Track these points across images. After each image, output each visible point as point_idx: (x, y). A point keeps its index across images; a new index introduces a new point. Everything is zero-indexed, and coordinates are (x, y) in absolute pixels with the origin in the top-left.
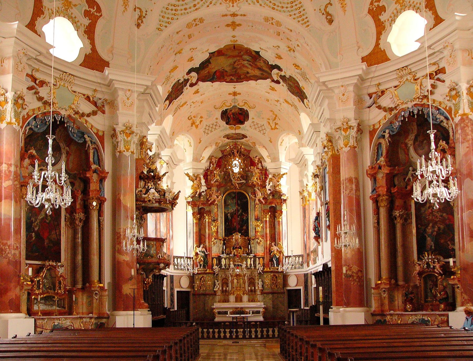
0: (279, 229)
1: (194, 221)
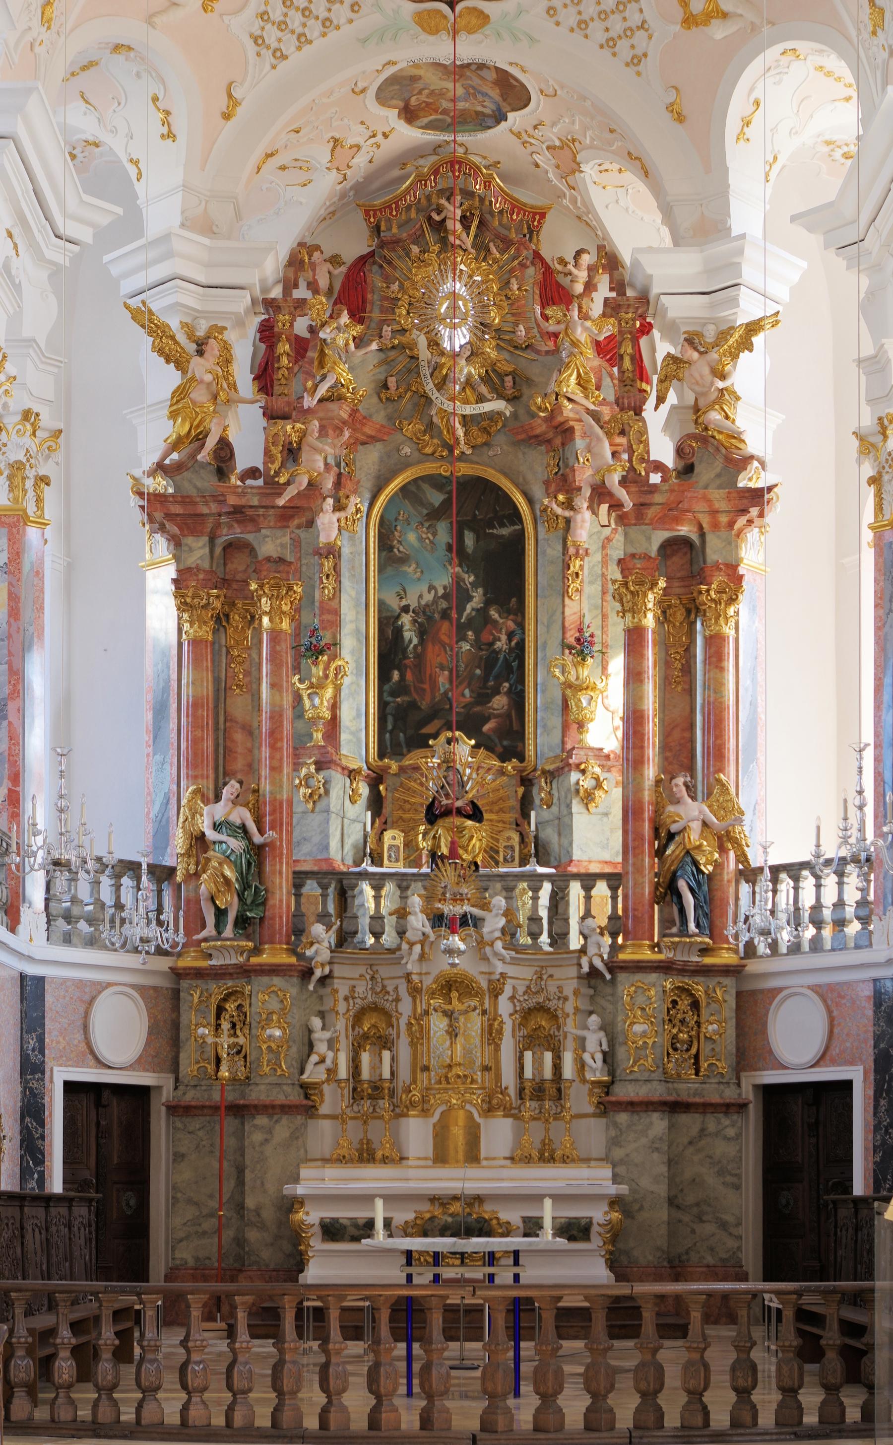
1: (186, 626)
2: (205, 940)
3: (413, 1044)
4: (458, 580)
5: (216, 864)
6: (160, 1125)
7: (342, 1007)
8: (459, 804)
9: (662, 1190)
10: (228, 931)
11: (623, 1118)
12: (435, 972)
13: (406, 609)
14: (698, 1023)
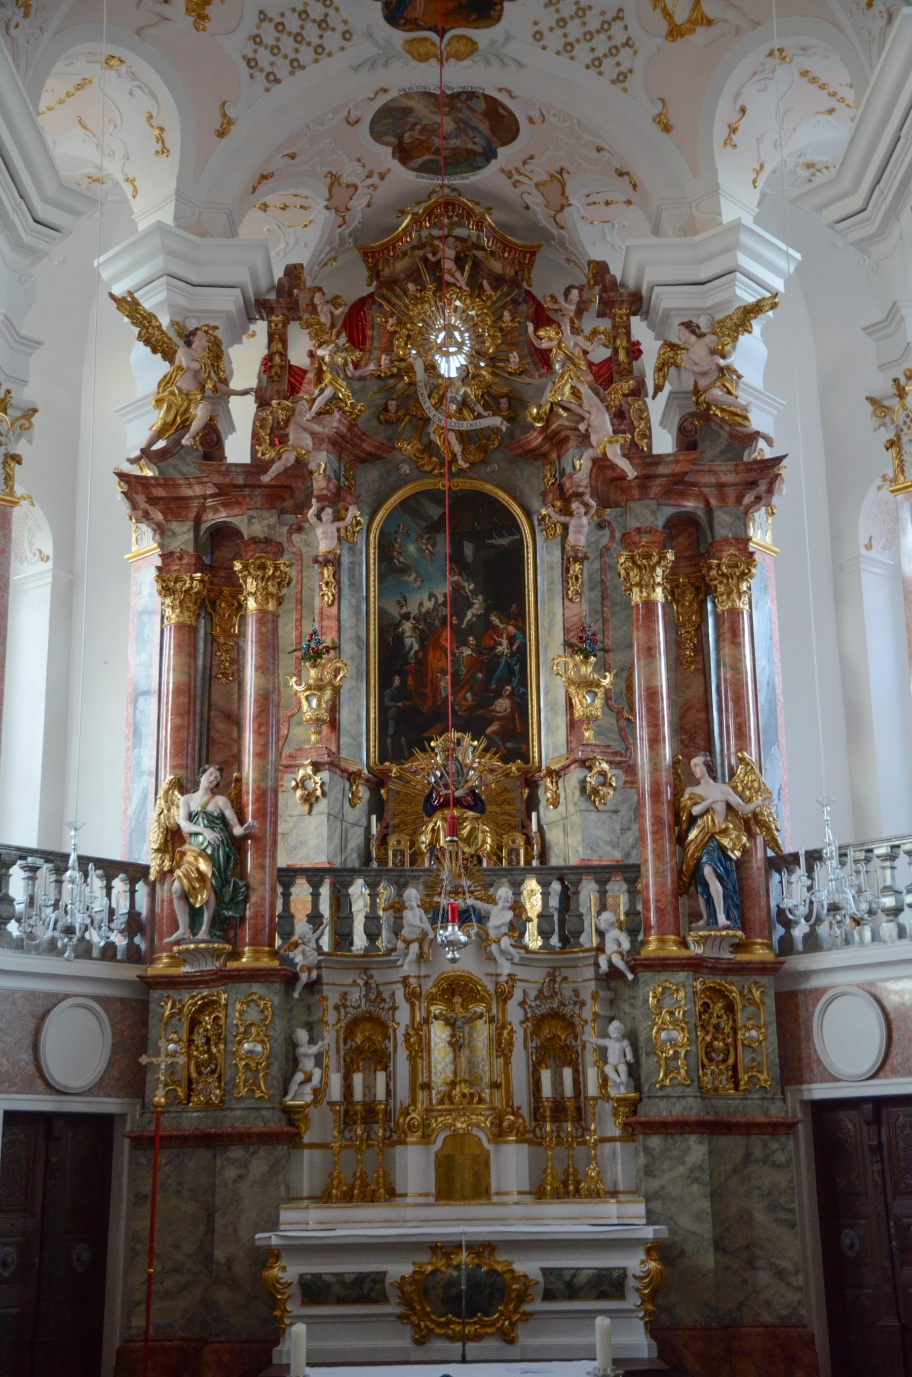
0: (737, 666)
2: (178, 943)
3: (412, 1059)
4: (457, 588)
5: (192, 859)
6: (123, 1155)
7: (331, 1017)
8: (458, 793)
9: (705, 1229)
10: (203, 933)
11: (655, 1142)
12: (435, 976)
13: (406, 617)
14: (735, 1030)
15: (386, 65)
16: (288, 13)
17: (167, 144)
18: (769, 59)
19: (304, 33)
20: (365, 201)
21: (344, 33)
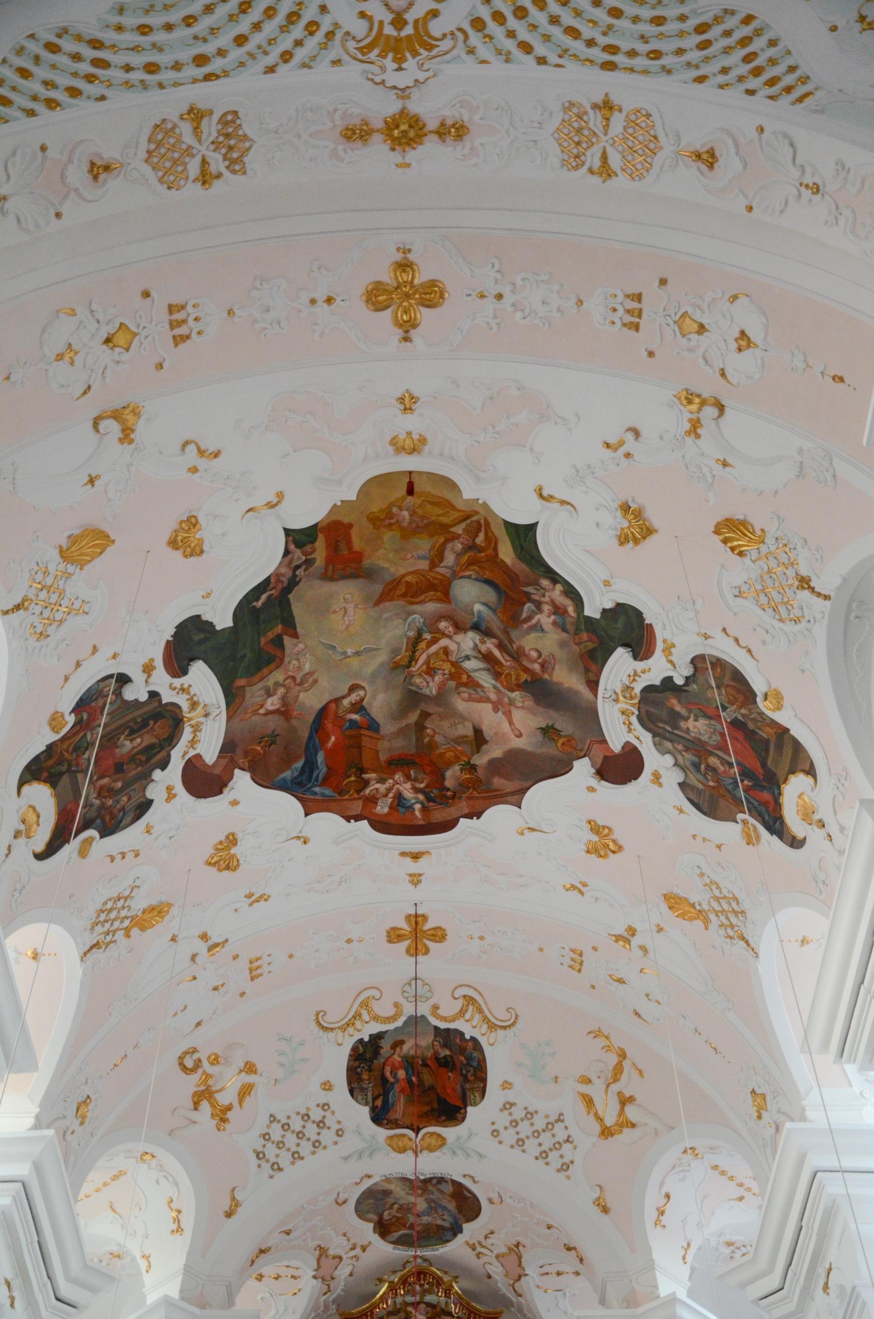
15: (371, 1155)
16: (293, 1116)
17: (182, 1226)
18: (684, 1156)
19: (305, 1131)
20: (348, 1270)
21: (337, 1131)
